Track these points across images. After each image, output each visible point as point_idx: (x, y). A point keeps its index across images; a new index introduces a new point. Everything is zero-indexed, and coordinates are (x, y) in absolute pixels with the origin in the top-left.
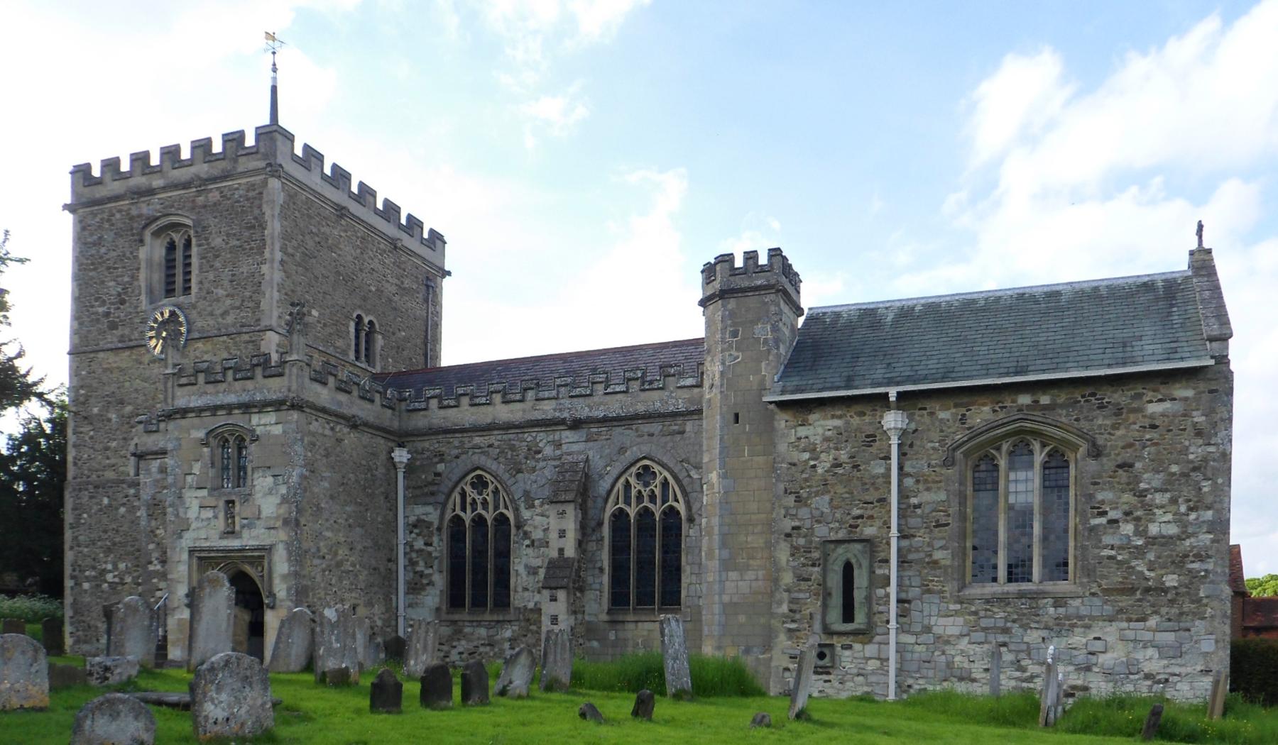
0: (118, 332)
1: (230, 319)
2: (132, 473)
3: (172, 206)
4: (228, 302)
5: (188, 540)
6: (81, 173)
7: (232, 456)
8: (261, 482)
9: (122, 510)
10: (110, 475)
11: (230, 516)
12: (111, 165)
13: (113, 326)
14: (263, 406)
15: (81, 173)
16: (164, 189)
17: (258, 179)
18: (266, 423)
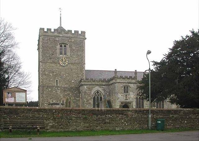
0: (52, 60)
1: (76, 61)
2: (56, 85)
3: (64, 40)
4: (76, 58)
5: (119, 100)
6: (42, 29)
7: (126, 90)
8: (131, 93)
9: (54, 91)
10: (51, 85)
11: (126, 97)
12: (49, 30)
13: (50, 58)
14: (131, 83)
15: (42, 29)
16: (62, 37)
17: (82, 40)
18: (132, 85)
